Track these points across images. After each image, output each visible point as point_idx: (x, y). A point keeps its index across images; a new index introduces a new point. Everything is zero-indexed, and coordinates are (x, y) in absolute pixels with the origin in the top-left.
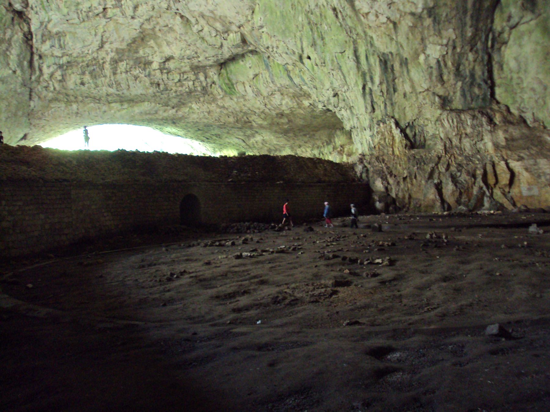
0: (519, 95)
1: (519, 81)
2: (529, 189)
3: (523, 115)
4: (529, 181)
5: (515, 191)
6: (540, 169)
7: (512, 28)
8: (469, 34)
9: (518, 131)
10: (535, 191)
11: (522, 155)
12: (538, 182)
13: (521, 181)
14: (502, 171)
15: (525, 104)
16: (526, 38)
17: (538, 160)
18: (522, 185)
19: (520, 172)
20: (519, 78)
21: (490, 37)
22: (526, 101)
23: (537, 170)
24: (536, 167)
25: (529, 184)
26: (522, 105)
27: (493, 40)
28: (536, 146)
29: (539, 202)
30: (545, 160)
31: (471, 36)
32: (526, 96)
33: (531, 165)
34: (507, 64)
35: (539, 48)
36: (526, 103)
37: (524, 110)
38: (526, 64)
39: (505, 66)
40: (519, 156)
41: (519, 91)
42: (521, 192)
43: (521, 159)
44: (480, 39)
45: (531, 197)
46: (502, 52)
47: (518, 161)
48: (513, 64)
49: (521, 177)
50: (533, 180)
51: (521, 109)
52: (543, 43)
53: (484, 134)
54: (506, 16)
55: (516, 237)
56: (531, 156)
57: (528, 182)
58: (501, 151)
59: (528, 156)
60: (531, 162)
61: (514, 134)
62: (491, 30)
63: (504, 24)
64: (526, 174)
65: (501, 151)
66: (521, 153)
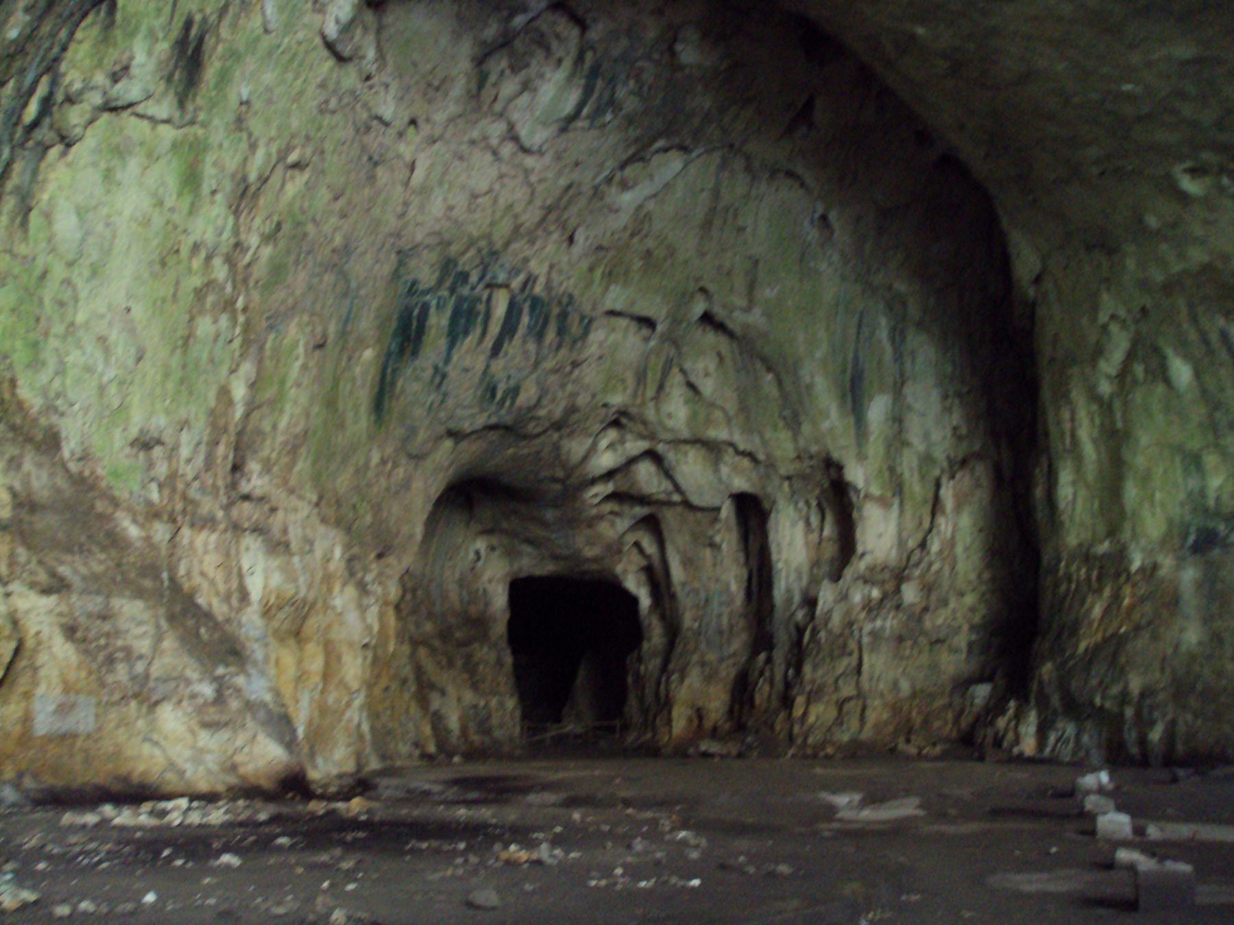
0: (53, 343)
1: (67, 295)
2: (63, 709)
3: (54, 419)
4: (72, 676)
6: (118, 633)
7: (111, 108)
8: (13, 34)
9: (44, 475)
10: (83, 719)
11: (63, 570)
12: (103, 685)
15: (63, 385)
16: (134, 164)
17: (117, 603)
18: (41, 690)
19: (44, 636)
20: (67, 282)
21: (42, 90)
22: (72, 373)
23: (108, 635)
24: (107, 627)
25: (68, 688)
27: (47, 103)
28: (104, 549)
29: (87, 760)
31: (13, 42)
33: (90, 616)
34: (48, 216)
35: (158, 221)
36: (68, 382)
37: (59, 402)
38: (107, 252)
39: (35, 218)
40: (53, 574)
41: (58, 329)
42: (27, 719)
43: (56, 586)
44: (22, 71)
45: (66, 738)
46: (43, 165)
47: (46, 591)
48: (66, 225)
49: (42, 658)
50: (83, 674)
52: (172, 210)
54: (112, 56)
55: (643, 884)
56: (95, 584)
57: (65, 682)
59: (84, 578)
60: (95, 603)
62: (51, 68)
63: (100, 78)
66: (61, 563)
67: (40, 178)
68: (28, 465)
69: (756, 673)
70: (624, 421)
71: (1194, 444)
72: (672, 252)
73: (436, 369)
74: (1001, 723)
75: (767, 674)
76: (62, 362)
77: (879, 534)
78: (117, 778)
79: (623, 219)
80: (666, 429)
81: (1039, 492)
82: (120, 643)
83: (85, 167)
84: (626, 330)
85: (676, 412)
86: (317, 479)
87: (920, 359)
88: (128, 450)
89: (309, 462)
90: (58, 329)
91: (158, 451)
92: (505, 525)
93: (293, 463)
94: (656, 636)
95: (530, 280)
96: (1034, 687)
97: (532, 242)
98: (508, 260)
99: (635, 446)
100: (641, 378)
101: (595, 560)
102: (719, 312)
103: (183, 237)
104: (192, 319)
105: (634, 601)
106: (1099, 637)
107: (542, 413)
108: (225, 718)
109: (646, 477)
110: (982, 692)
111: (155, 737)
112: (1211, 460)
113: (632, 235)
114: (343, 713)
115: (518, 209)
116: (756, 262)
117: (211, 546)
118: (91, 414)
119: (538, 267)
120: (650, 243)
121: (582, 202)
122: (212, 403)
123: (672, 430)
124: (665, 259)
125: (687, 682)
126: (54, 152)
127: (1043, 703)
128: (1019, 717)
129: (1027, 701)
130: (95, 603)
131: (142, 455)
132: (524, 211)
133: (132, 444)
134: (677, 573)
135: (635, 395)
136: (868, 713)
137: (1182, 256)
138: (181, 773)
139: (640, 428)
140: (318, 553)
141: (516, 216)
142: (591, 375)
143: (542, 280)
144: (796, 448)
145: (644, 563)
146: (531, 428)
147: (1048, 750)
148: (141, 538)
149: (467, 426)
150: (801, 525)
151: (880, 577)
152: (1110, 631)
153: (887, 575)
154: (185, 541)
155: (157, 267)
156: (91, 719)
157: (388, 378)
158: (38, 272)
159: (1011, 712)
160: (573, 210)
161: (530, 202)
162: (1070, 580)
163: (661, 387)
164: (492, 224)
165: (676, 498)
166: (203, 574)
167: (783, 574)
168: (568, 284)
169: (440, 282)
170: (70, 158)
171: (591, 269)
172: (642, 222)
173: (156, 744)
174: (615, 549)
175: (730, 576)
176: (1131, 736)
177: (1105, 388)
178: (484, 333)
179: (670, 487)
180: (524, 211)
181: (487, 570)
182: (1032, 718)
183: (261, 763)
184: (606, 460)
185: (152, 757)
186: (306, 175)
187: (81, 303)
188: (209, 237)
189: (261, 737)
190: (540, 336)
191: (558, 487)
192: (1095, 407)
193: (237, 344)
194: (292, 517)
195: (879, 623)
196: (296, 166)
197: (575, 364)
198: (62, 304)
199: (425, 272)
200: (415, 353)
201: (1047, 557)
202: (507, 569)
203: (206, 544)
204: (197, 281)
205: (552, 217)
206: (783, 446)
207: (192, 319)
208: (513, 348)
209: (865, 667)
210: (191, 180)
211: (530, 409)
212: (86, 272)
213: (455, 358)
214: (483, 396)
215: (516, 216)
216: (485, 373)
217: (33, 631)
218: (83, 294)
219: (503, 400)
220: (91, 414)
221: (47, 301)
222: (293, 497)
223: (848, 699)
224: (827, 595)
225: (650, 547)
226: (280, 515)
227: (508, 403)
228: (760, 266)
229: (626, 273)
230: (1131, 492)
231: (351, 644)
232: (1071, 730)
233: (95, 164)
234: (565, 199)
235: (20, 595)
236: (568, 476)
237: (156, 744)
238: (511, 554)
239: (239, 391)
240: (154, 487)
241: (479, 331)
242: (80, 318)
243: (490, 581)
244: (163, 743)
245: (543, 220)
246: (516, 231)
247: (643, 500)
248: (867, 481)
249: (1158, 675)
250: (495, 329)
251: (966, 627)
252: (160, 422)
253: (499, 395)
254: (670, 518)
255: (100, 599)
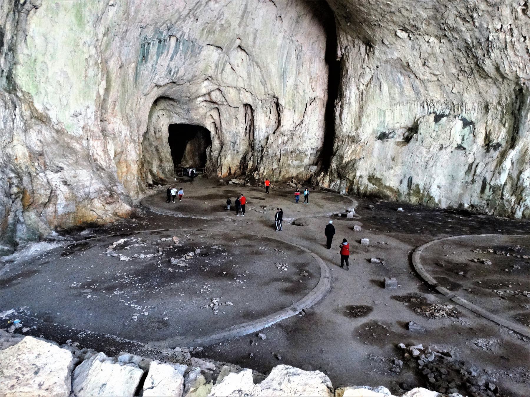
0: (42, 85)
1: (44, 68)
3: (47, 111)
5: (50, 209)
9: (49, 134)
13: (59, 197)
14: (39, 187)
17: (78, 171)
19: (58, 186)
22: (50, 95)
23: (77, 182)
24: (76, 179)
26: (46, 100)
30: (85, 171)
32: (50, 89)
33: (71, 177)
36: (49, 98)
38: (55, 50)
42: (56, 212)
48: (39, 41)
49: (58, 192)
51: (45, 104)
53: (15, 133)
58: (38, 160)
61: (47, 137)
64: (64, 189)
65: (38, 160)
67: (28, 23)
68: (44, 131)
69: (248, 158)
70: (210, 79)
71: (383, 108)
72: (230, 25)
73: (153, 66)
74: (319, 178)
75: (252, 159)
76: (46, 91)
77: (288, 120)
78: (84, 223)
79: (216, 13)
80: (223, 82)
81: (337, 114)
82: (81, 184)
83: (44, 17)
84: (213, 51)
85: (228, 77)
86: (121, 112)
87: (304, 66)
88: (71, 118)
89: (119, 107)
90: (43, 80)
91: (80, 117)
92: (168, 108)
93: (115, 107)
94: (216, 143)
95: (183, 34)
96: (329, 170)
97: (184, 21)
98: (176, 27)
99: (212, 87)
100: (217, 66)
101: (197, 120)
102: (243, 45)
103: (80, 41)
104: (86, 70)
105: (209, 132)
106: (349, 159)
107: (185, 78)
108: (113, 200)
109: (215, 96)
110: (314, 168)
111: (93, 209)
112: (388, 113)
113: (218, 19)
114: (132, 181)
115: (181, 10)
116: (257, 31)
117: (99, 145)
118: (58, 108)
119: (186, 30)
120: (223, 22)
121: (202, 7)
122: (95, 98)
123: (226, 83)
124: (227, 28)
125: (227, 159)
126: (32, 12)
127: (331, 174)
128: (324, 177)
129: (327, 173)
130: (72, 173)
131: (75, 119)
132: (183, 11)
133: (72, 116)
134: (224, 125)
135: (214, 72)
136: (281, 173)
137: (392, 53)
138: (102, 218)
139: (215, 82)
140: (123, 136)
141: (180, 13)
142: (201, 65)
143: (187, 34)
144: (265, 92)
145: (213, 121)
146: (182, 82)
147: (331, 187)
148: (80, 148)
149: (162, 83)
150: (264, 114)
151: (287, 133)
152: (353, 158)
153: (289, 133)
154: (91, 145)
155: (73, 53)
156: (75, 207)
157: (138, 71)
158: (33, 60)
159: (322, 175)
160: (199, 10)
161: (185, 8)
162: (343, 141)
163: (223, 70)
164: (172, 16)
165: (225, 103)
166: (97, 154)
167: (257, 130)
168: (195, 35)
169: (154, 35)
170: (37, 14)
171: (203, 30)
172: (221, 15)
173: (94, 211)
174: (205, 117)
175: (241, 127)
176: (355, 187)
177: (361, 87)
178: (168, 52)
179: (224, 100)
180: (183, 11)
181: (163, 122)
182: (328, 178)
183: (124, 211)
184: (204, 91)
185: (93, 215)
186: (115, 8)
187: (50, 69)
188: (88, 40)
189: (123, 204)
190: (186, 54)
191: (188, 98)
192: (357, 92)
193: (100, 74)
194: (115, 125)
195: (286, 147)
196: (112, 5)
197: (196, 62)
198: (43, 70)
199: (149, 33)
200: (146, 62)
201: (337, 133)
202: (168, 121)
203: (97, 144)
204: (86, 56)
205: (191, 13)
206: (260, 91)
207: (86, 70)
208: (177, 58)
209: (281, 160)
210: (80, 18)
211: (182, 77)
212: (49, 57)
213: (159, 62)
214: (167, 74)
215: (180, 13)
216: (168, 66)
217: (54, 185)
218: (49, 65)
219: (173, 75)
220: (58, 108)
221: (37, 69)
222: (115, 118)
223: (275, 169)
224: (271, 138)
225: (216, 117)
226: (111, 125)
227: (175, 76)
228: (258, 32)
229: (214, 32)
230: (364, 120)
231: (133, 161)
232: (338, 182)
233: (47, 16)
234: (196, 7)
235: (49, 174)
236: (191, 96)
237: (94, 211)
238: (170, 117)
239: (102, 92)
240: (80, 129)
241: (166, 52)
242: (50, 75)
243: (163, 126)
244: (95, 210)
245: (188, 14)
246: (179, 18)
247: (214, 103)
248: (285, 104)
249: (364, 172)
250: (171, 51)
251: (310, 149)
252: (79, 108)
253: (172, 73)
254: (222, 108)
255: (73, 172)
